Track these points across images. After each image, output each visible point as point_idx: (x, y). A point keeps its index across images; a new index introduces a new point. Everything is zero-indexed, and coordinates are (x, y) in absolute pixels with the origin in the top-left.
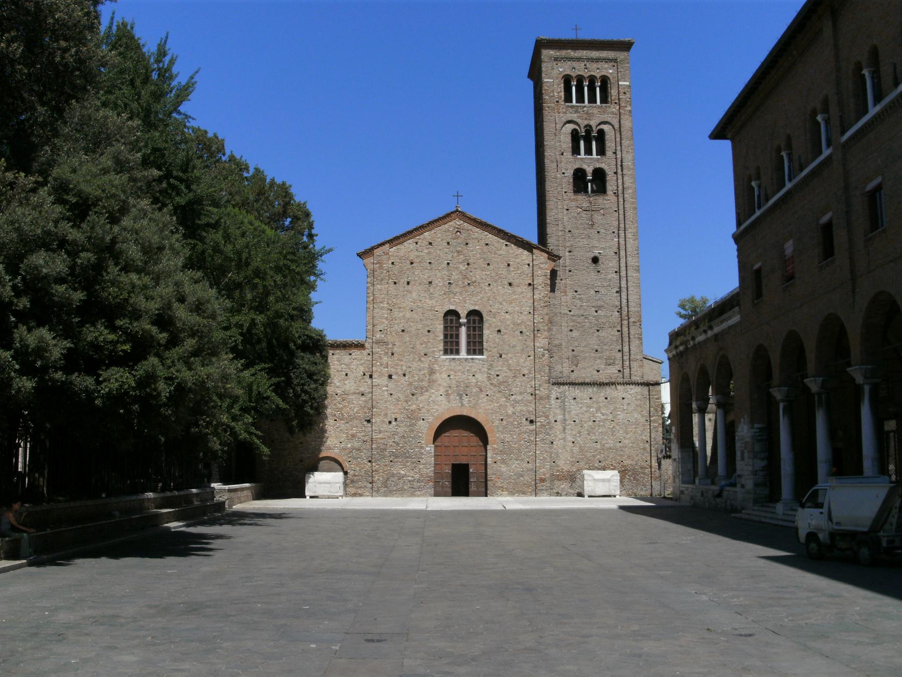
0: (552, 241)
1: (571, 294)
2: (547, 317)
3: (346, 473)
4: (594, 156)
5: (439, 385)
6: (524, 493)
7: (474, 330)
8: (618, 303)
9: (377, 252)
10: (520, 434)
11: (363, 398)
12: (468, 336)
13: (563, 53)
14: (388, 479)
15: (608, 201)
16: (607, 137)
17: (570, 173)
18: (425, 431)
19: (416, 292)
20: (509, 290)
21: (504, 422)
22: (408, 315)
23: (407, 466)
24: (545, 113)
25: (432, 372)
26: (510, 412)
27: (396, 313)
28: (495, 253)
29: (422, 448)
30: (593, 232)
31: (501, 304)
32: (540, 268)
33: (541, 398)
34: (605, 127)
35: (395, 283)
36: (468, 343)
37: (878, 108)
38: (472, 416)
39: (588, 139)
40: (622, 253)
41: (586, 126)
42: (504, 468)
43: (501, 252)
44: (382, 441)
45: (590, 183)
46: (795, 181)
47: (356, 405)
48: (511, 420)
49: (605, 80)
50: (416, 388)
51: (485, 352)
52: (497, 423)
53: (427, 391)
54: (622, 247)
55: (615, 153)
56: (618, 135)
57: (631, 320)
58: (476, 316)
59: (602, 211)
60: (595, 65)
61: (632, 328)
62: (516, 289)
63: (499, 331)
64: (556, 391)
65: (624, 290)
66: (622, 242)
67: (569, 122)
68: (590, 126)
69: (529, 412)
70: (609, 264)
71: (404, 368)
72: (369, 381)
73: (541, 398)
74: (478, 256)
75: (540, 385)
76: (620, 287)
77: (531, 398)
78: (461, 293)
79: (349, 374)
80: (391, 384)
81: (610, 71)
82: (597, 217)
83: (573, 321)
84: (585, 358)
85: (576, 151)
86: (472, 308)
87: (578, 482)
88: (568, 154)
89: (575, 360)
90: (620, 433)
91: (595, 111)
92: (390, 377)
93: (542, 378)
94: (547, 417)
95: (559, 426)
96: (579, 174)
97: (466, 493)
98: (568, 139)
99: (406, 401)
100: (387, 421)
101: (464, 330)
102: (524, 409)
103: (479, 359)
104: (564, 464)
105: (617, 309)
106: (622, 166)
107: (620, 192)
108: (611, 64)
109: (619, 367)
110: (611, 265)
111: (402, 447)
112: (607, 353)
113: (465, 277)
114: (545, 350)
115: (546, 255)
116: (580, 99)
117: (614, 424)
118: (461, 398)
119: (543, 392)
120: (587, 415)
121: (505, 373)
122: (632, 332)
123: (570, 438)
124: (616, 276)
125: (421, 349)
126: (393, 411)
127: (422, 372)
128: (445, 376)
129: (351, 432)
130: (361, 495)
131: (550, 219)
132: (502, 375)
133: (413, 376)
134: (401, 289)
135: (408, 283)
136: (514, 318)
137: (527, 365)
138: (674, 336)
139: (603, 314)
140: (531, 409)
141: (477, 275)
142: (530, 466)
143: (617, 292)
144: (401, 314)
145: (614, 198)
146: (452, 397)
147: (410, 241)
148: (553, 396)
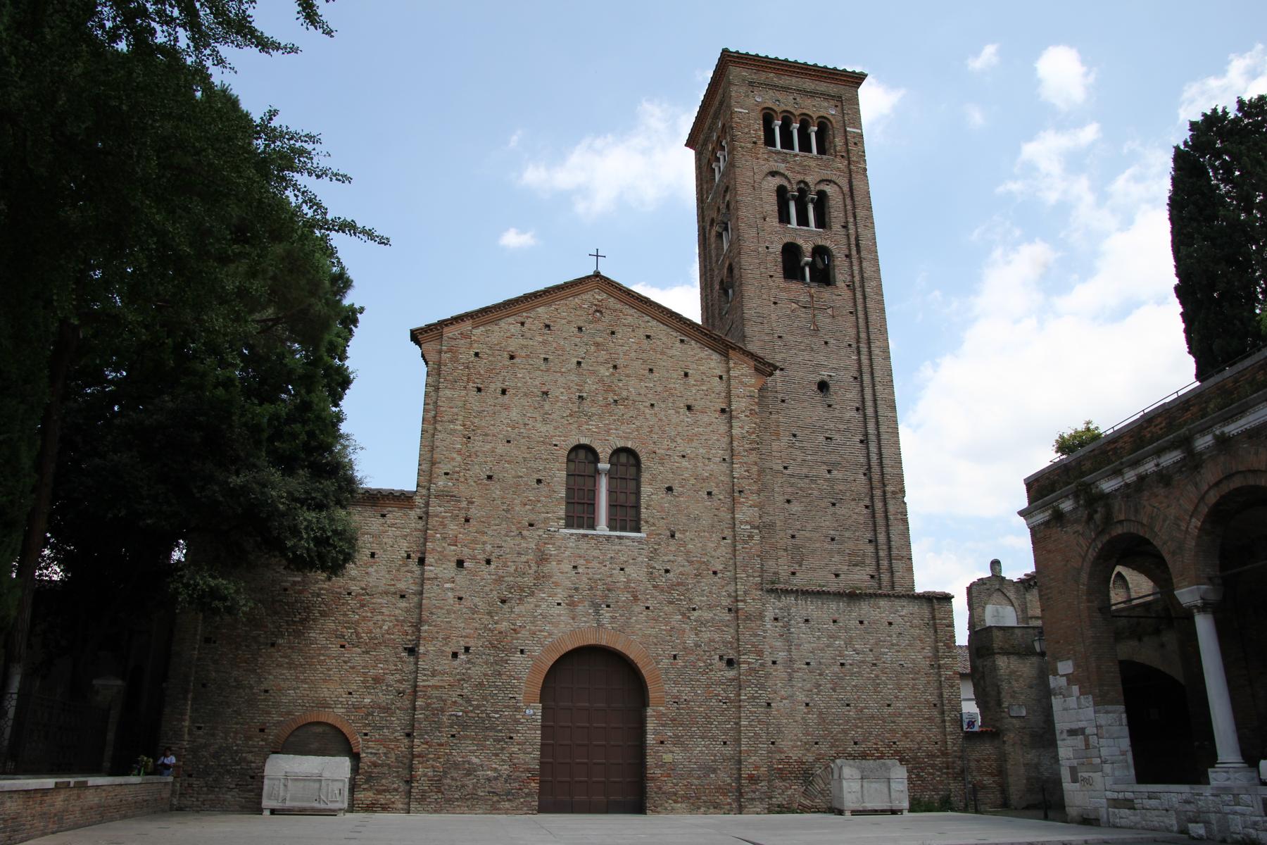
1: (786, 438)
2: (755, 469)
3: (355, 757)
5: (556, 584)
6: (717, 807)
8: (863, 460)
9: (449, 332)
11: (403, 604)
13: (763, 77)
14: (445, 773)
15: (838, 296)
16: (832, 203)
17: (777, 248)
20: (688, 418)
21: (680, 662)
22: (501, 448)
24: (738, 155)
25: (543, 559)
26: (690, 643)
27: (477, 444)
28: (663, 353)
29: (517, 709)
31: (673, 441)
32: (741, 382)
33: (748, 618)
34: (828, 189)
35: (479, 390)
36: (612, 506)
38: (619, 647)
39: (797, 201)
40: (867, 378)
43: (674, 352)
47: (388, 616)
48: (692, 658)
50: (510, 588)
51: (644, 527)
52: (665, 662)
53: (532, 594)
54: (866, 369)
56: (848, 201)
57: (889, 488)
58: (627, 458)
59: (829, 311)
60: (808, 102)
61: (891, 503)
62: (700, 416)
63: (670, 489)
64: (773, 607)
65: (872, 438)
66: (865, 361)
67: (773, 174)
68: (806, 184)
69: (725, 643)
70: (846, 395)
71: (488, 548)
72: (416, 568)
73: (748, 618)
74: (633, 355)
76: (866, 434)
77: (728, 617)
79: (379, 552)
80: (462, 578)
82: (823, 320)
83: (792, 485)
85: (784, 218)
86: (620, 444)
87: (819, 785)
88: (774, 221)
91: (813, 164)
92: (460, 563)
94: (760, 653)
95: (780, 672)
96: (791, 252)
98: (773, 199)
99: (490, 613)
100: (449, 650)
101: (604, 483)
102: (717, 637)
103: (633, 539)
104: (792, 747)
106: (858, 245)
107: (857, 284)
108: (832, 102)
109: (870, 570)
110: (849, 396)
111: (478, 707)
112: (849, 545)
113: (609, 389)
114: (753, 527)
115: (752, 363)
118: (597, 612)
119: (749, 605)
120: (830, 652)
121: (680, 567)
123: (801, 697)
125: (523, 513)
127: (524, 558)
128: (567, 567)
129: (372, 672)
130: (385, 808)
134: (490, 401)
135: (504, 392)
136: (696, 466)
137: (719, 555)
140: (729, 638)
141: (631, 388)
142: (728, 751)
143: (862, 442)
144: (488, 446)
145: (847, 294)
146: (580, 608)
147: (510, 320)
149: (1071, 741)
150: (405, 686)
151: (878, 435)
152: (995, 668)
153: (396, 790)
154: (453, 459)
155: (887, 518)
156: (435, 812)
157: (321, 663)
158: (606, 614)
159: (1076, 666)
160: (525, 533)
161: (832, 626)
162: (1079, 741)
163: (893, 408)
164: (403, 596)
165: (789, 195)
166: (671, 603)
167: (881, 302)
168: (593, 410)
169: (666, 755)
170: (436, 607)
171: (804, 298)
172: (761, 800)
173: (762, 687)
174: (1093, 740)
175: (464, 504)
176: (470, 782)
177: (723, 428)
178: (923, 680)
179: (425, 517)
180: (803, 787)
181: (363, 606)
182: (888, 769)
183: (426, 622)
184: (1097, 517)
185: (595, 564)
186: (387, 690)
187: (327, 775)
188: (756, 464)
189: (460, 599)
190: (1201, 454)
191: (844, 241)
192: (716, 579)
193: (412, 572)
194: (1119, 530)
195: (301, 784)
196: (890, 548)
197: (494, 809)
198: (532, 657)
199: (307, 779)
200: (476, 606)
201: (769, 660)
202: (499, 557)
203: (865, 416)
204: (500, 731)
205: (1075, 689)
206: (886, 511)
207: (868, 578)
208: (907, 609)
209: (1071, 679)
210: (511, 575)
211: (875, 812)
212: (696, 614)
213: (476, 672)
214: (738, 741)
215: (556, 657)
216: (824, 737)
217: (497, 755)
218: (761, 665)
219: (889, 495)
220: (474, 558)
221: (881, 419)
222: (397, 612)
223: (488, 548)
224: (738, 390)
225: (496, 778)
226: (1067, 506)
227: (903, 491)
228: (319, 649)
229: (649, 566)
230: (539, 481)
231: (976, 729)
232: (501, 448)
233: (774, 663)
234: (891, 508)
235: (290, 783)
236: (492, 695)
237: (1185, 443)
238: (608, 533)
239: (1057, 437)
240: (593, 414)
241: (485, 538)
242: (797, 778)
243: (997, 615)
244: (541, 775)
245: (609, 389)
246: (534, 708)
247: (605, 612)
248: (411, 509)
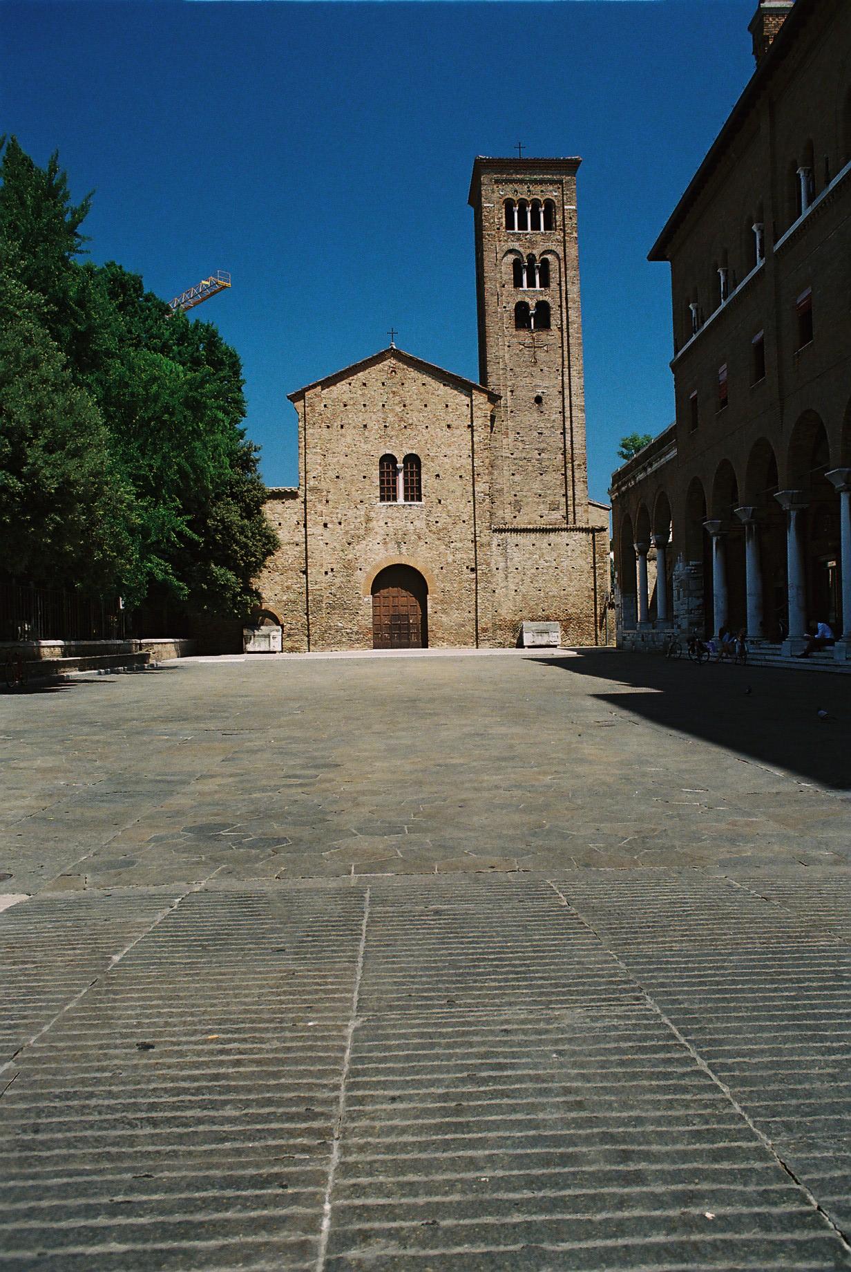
0: (492, 380)
1: (512, 435)
3: (283, 627)
4: (538, 288)
11: (298, 548)
16: (551, 267)
18: (362, 581)
19: (350, 435)
20: (448, 433)
22: (343, 460)
25: (369, 520)
26: (450, 560)
27: (330, 459)
30: (536, 370)
34: (549, 257)
36: (406, 489)
37: (810, 210)
40: (567, 392)
42: (445, 619)
45: (533, 318)
46: (729, 299)
49: (549, 204)
50: (353, 537)
54: (566, 386)
55: (560, 284)
56: (563, 265)
60: (539, 188)
62: (455, 431)
64: (498, 537)
66: (566, 381)
67: (511, 251)
69: (470, 560)
70: (553, 404)
76: (564, 429)
80: (327, 533)
81: (553, 193)
82: (541, 355)
84: (528, 503)
85: (518, 283)
86: (409, 452)
89: (517, 506)
90: (564, 581)
91: (539, 238)
92: (325, 525)
93: (482, 525)
94: (488, 564)
95: (501, 574)
96: (521, 308)
100: (323, 571)
101: (401, 476)
102: (464, 556)
109: (563, 512)
112: (551, 498)
113: (401, 420)
116: (523, 226)
117: (558, 571)
120: (530, 563)
121: (444, 520)
122: (576, 475)
124: (560, 417)
125: (357, 496)
131: (489, 357)
132: (442, 521)
138: (618, 478)
141: (413, 417)
148: (495, 543)
158: (404, 547)
169: (438, 617)
171: (528, 341)
173: (490, 582)
179: (305, 502)
213: (337, 581)
224: (477, 413)
232: (343, 460)
245: (401, 420)
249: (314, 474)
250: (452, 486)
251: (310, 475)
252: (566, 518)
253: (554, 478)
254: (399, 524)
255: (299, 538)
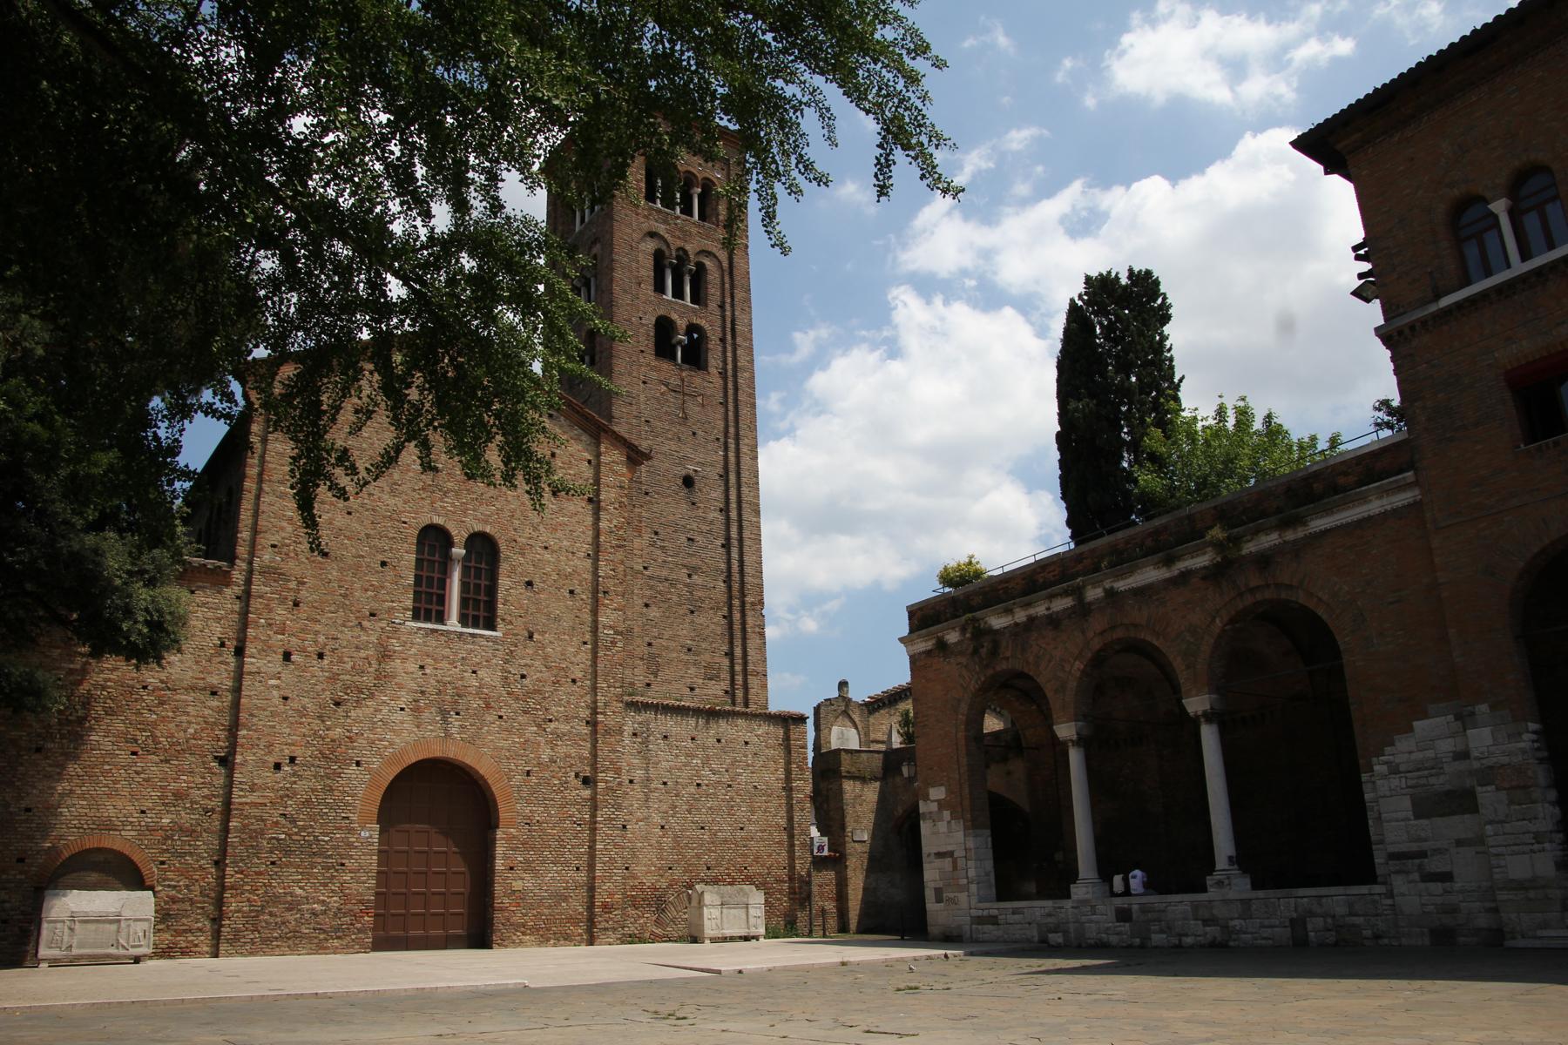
5: (400, 686)
6: (567, 938)
7: (478, 577)
8: (723, 566)
10: (563, 806)
11: (215, 703)
12: (464, 586)
15: (709, 383)
16: (710, 277)
17: (650, 320)
21: (534, 779)
23: (308, 876)
25: (385, 655)
26: (545, 758)
29: (351, 831)
31: (535, 529)
34: (708, 263)
36: (464, 602)
38: (468, 761)
41: (678, 249)
44: (255, 812)
50: (346, 688)
51: (501, 625)
52: (518, 779)
54: (732, 467)
55: (722, 307)
56: (727, 279)
57: (749, 599)
61: (749, 613)
63: (530, 584)
64: (631, 722)
65: (735, 543)
66: (732, 459)
67: (652, 235)
68: (685, 252)
69: (581, 758)
71: (322, 639)
75: (606, 705)
76: (728, 538)
77: (586, 730)
78: (457, 493)
80: (288, 674)
82: (693, 408)
83: (651, 588)
84: (670, 662)
85: (660, 288)
86: (478, 527)
88: (648, 288)
89: (654, 665)
90: (742, 812)
91: (694, 230)
92: (287, 656)
94: (618, 771)
95: (637, 791)
96: (664, 327)
97: (480, 936)
98: (650, 263)
99: (320, 717)
100: (272, 760)
103: (488, 639)
104: (647, 873)
105: (723, 577)
106: (733, 330)
107: (730, 373)
109: (725, 685)
111: (303, 828)
112: (707, 657)
114: (617, 633)
120: (686, 773)
121: (538, 672)
123: (657, 819)
125: (363, 600)
126: (288, 737)
127: (363, 654)
130: (185, 953)
133: (341, 661)
139: (700, 581)
145: (718, 381)
146: (426, 715)
148: (628, 730)
149: (938, 862)
150: (216, 803)
151: (741, 540)
152: (840, 791)
153: (200, 930)
154: (283, 529)
155: (744, 630)
156: (252, 954)
157: (105, 773)
159: (949, 792)
160: (365, 623)
161: (690, 744)
162: (947, 863)
163: (757, 513)
164: (214, 693)
165: (666, 262)
166: (525, 712)
167: (752, 396)
168: (449, 485)
170: (258, 708)
172: (614, 929)
173: (619, 807)
174: (961, 863)
175: (293, 585)
176: (291, 917)
177: (589, 520)
178: (775, 803)
179: (246, 597)
180: (664, 913)
181: (162, 703)
182: (746, 895)
183: (245, 726)
184: (984, 651)
185: (444, 664)
186: (192, 808)
187: (127, 914)
188: (622, 562)
189: (286, 698)
190: (1090, 604)
191: (719, 323)
192: (575, 688)
193: (227, 664)
194: (1004, 666)
195: (92, 927)
196: (745, 663)
197: (321, 948)
198: (369, 770)
199: (101, 920)
200: (304, 708)
201: (625, 778)
202: (333, 650)
203: (728, 518)
204: (330, 857)
205: (947, 814)
206: (744, 623)
207: (721, 693)
208: (763, 729)
209: (942, 805)
210: (348, 673)
211: (732, 939)
212: (552, 725)
214: (591, 867)
215: (397, 770)
216: (677, 862)
217: (325, 885)
218: (620, 784)
219: (748, 606)
220: (303, 650)
221: (745, 524)
222: (207, 712)
223: (322, 639)
225: (324, 912)
226: (952, 637)
227: (761, 602)
228: (102, 756)
229: (504, 670)
230: (383, 564)
231: (826, 853)
233: (631, 782)
234: (750, 621)
235: (77, 926)
236: (322, 814)
237: (1078, 592)
238: (459, 629)
239: (941, 568)
240: (449, 491)
241: (318, 627)
242: (649, 905)
243: (842, 736)
244: (376, 908)
246: (371, 829)
247: (453, 718)
248: (227, 586)
249: (275, 539)
250: (556, 608)
251: (265, 540)
252: (731, 693)
253: (713, 622)
254: (449, 672)
255: (221, 677)
